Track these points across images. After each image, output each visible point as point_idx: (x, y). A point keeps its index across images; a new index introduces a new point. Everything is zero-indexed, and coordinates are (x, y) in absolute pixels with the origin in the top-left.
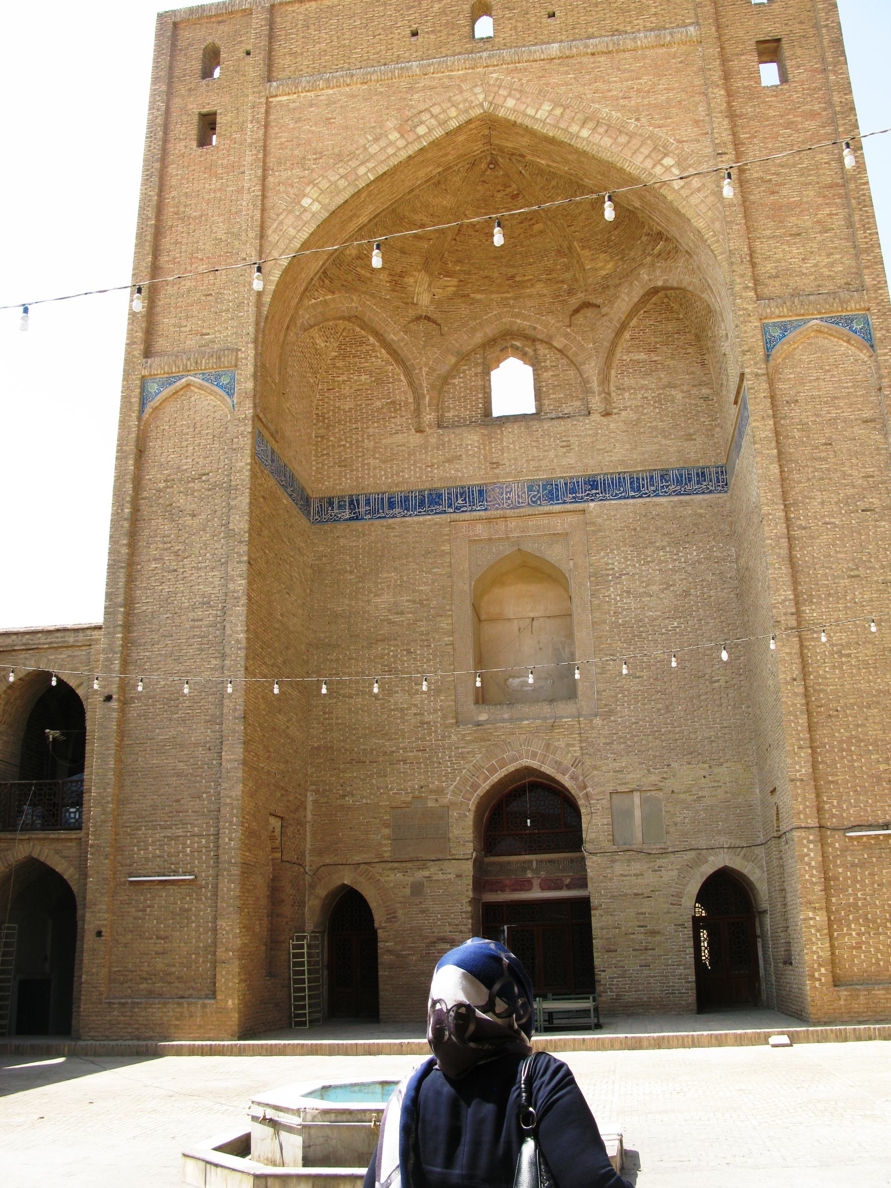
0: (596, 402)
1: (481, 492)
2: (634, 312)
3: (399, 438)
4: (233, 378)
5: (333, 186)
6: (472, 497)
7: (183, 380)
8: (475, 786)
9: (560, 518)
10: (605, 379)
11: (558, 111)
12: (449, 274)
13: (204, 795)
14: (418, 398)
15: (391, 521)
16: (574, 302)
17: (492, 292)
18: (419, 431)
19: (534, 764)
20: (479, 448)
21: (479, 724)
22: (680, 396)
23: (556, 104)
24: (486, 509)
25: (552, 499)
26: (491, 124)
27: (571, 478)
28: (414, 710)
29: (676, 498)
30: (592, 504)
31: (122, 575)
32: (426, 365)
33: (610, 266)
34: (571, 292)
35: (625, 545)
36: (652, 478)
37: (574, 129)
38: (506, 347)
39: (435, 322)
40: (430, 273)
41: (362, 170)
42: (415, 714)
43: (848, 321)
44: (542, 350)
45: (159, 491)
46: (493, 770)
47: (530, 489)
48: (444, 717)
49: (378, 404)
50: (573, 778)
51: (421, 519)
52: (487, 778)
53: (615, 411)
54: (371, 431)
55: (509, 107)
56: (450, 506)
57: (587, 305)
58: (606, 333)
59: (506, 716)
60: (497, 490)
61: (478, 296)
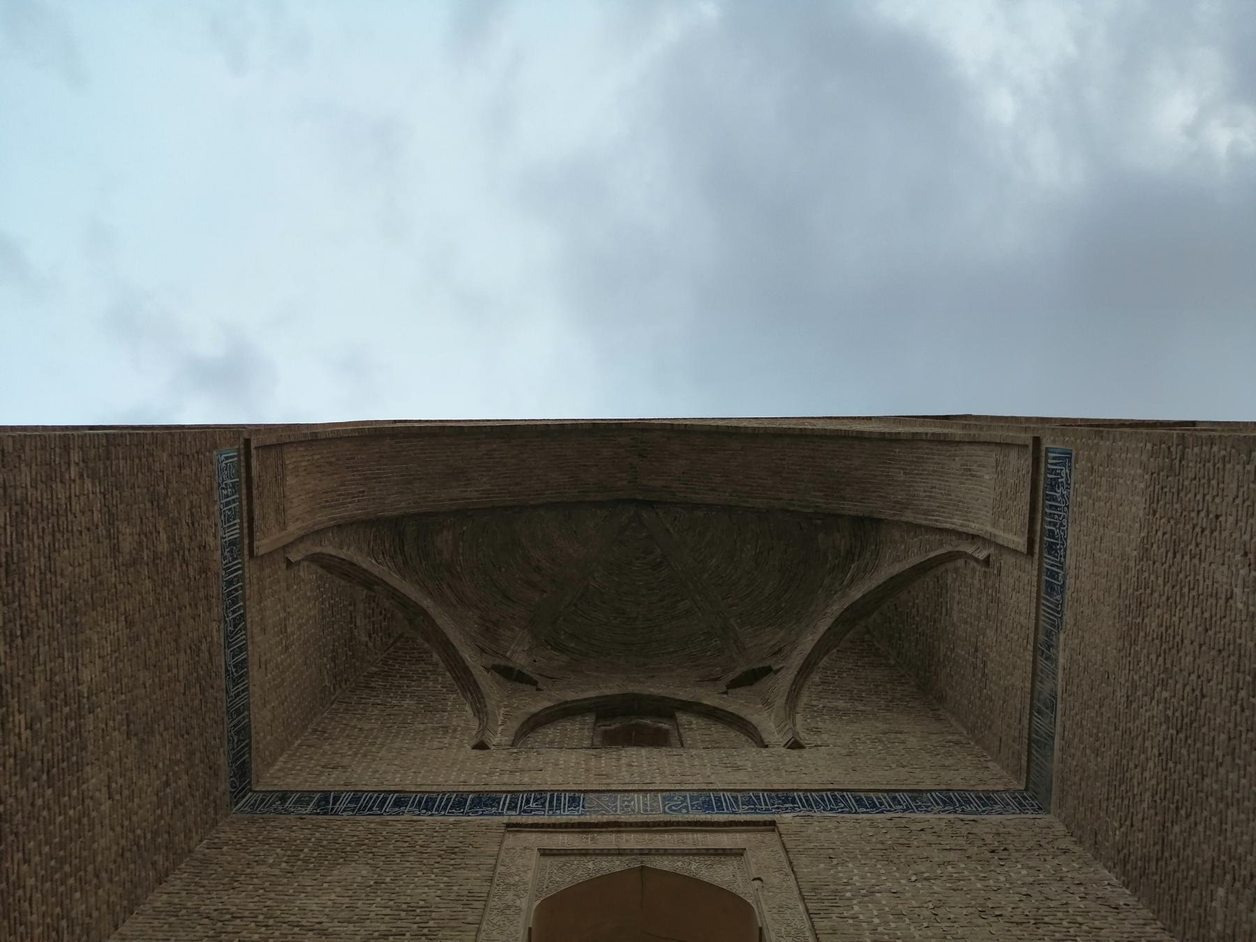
2: (821, 648)
51: (452, 819)
58: (784, 680)
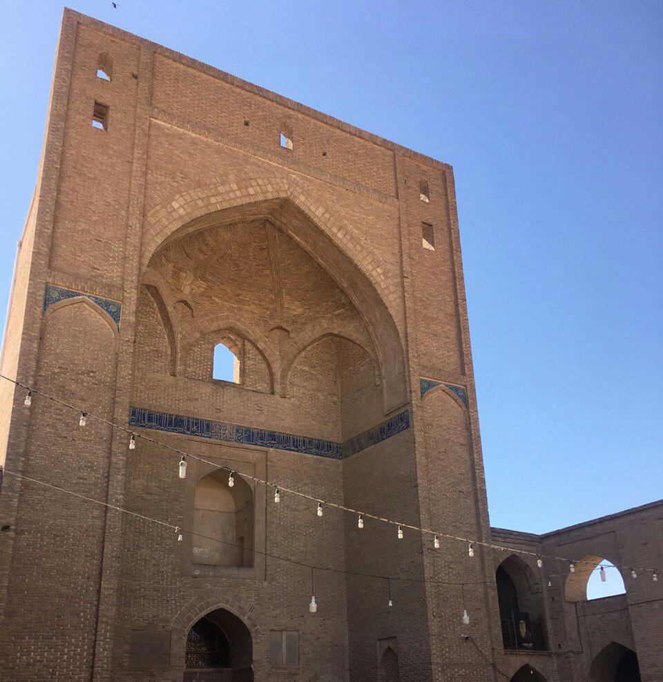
0: (277, 387)
1: (208, 425)
3: (159, 376)
4: (119, 309)
5: (194, 202)
6: (202, 427)
7: (80, 297)
8: (190, 619)
9: (252, 453)
10: (284, 377)
11: (327, 216)
12: (204, 279)
13: (82, 614)
14: (174, 354)
15: (148, 430)
16: (272, 324)
17: (225, 300)
18: (175, 376)
19: (227, 607)
20: (209, 396)
21: (195, 577)
22: (322, 398)
23: (327, 211)
24: (210, 437)
25: (249, 440)
26: (285, 205)
27: (261, 430)
28: (153, 562)
29: (316, 457)
30: (271, 449)
31: (24, 432)
32: (181, 333)
33: (300, 310)
34: (272, 317)
35: (288, 478)
36: (304, 441)
37: (335, 230)
38: (225, 337)
39: (190, 308)
40: (195, 276)
41: (213, 200)
42: (154, 565)
43: (457, 390)
44: (248, 346)
45: (54, 374)
46: (201, 609)
47: (237, 431)
48: (173, 569)
49: (147, 349)
50: (249, 619)
51: (169, 433)
52: (197, 614)
53: (288, 396)
54: (140, 365)
55: (300, 200)
56: (188, 430)
57: (280, 328)
59: (211, 573)
60: (218, 427)
61: (217, 300)
